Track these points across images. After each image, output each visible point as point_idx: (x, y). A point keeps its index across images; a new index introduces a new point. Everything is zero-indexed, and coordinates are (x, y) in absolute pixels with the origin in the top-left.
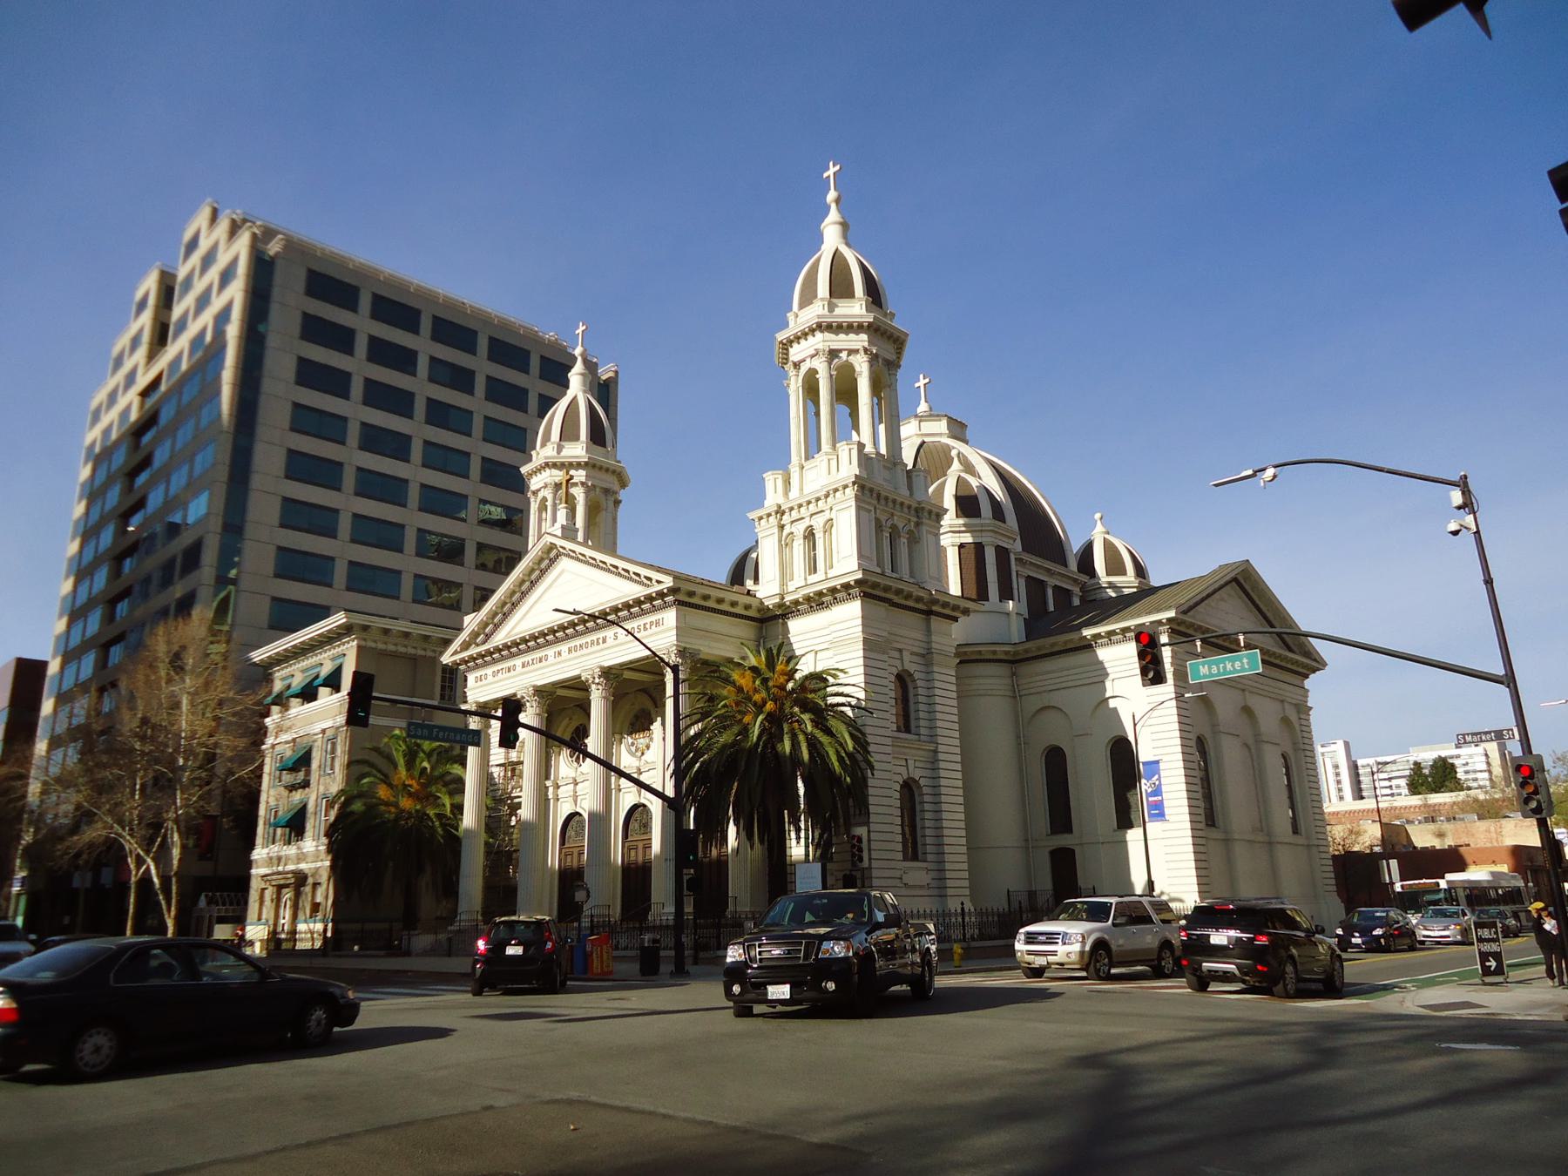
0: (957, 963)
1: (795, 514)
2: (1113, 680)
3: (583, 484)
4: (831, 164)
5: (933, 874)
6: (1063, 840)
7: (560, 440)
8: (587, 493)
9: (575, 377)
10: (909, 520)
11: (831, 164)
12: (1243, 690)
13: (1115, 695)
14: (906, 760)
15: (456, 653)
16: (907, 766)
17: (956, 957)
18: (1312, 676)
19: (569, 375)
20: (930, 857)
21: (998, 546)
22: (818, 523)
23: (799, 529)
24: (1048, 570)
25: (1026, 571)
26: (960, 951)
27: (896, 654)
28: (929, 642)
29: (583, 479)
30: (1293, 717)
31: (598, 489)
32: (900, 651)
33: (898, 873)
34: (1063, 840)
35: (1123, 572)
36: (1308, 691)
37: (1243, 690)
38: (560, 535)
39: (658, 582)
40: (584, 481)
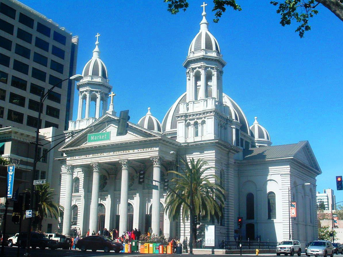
0: (257, 254)
1: (191, 117)
4: (204, 3)
5: (227, 230)
6: (250, 221)
11: (204, 3)
12: (303, 180)
15: (64, 148)
17: (257, 253)
20: (226, 225)
22: (199, 121)
23: (192, 122)
26: (258, 251)
28: (228, 160)
34: (250, 221)
35: (263, 137)
36: (316, 180)
37: (303, 180)
38: (111, 114)
39: (155, 136)
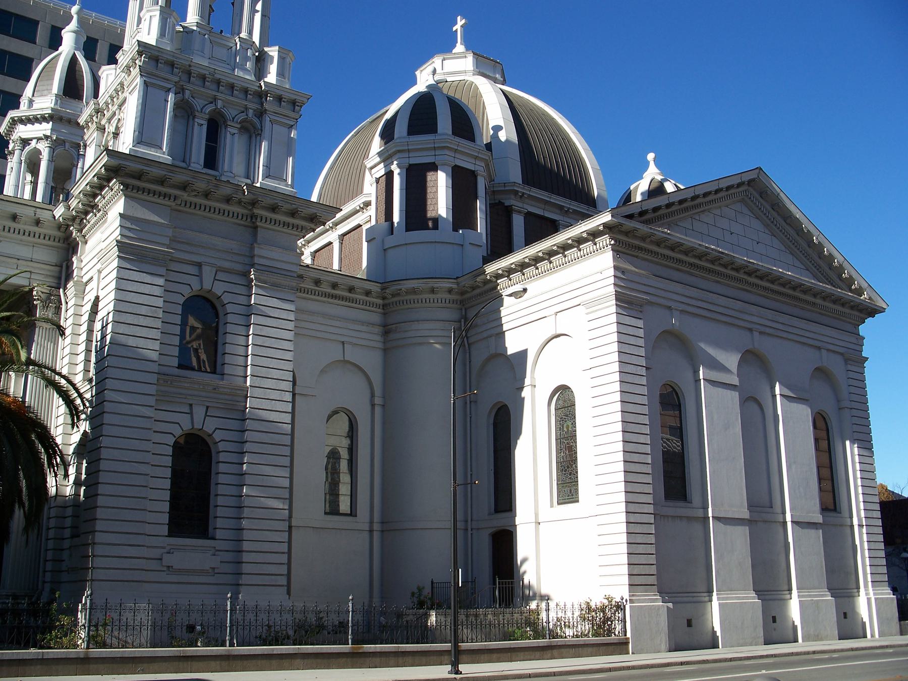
2: (556, 313)
3: (47, 137)
7: (33, 95)
8: (52, 149)
9: (68, 37)
10: (247, 109)
12: (750, 330)
13: (559, 332)
14: (191, 405)
16: (191, 413)
18: (869, 320)
19: (63, 32)
21: (456, 166)
24: (561, 208)
25: (526, 206)
27: (193, 270)
29: (48, 133)
30: (836, 366)
31: (67, 145)
32: (199, 265)
33: (156, 553)
40: (49, 134)
